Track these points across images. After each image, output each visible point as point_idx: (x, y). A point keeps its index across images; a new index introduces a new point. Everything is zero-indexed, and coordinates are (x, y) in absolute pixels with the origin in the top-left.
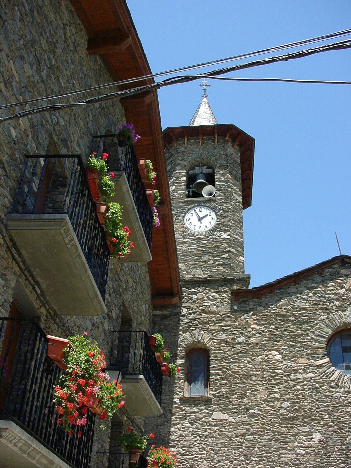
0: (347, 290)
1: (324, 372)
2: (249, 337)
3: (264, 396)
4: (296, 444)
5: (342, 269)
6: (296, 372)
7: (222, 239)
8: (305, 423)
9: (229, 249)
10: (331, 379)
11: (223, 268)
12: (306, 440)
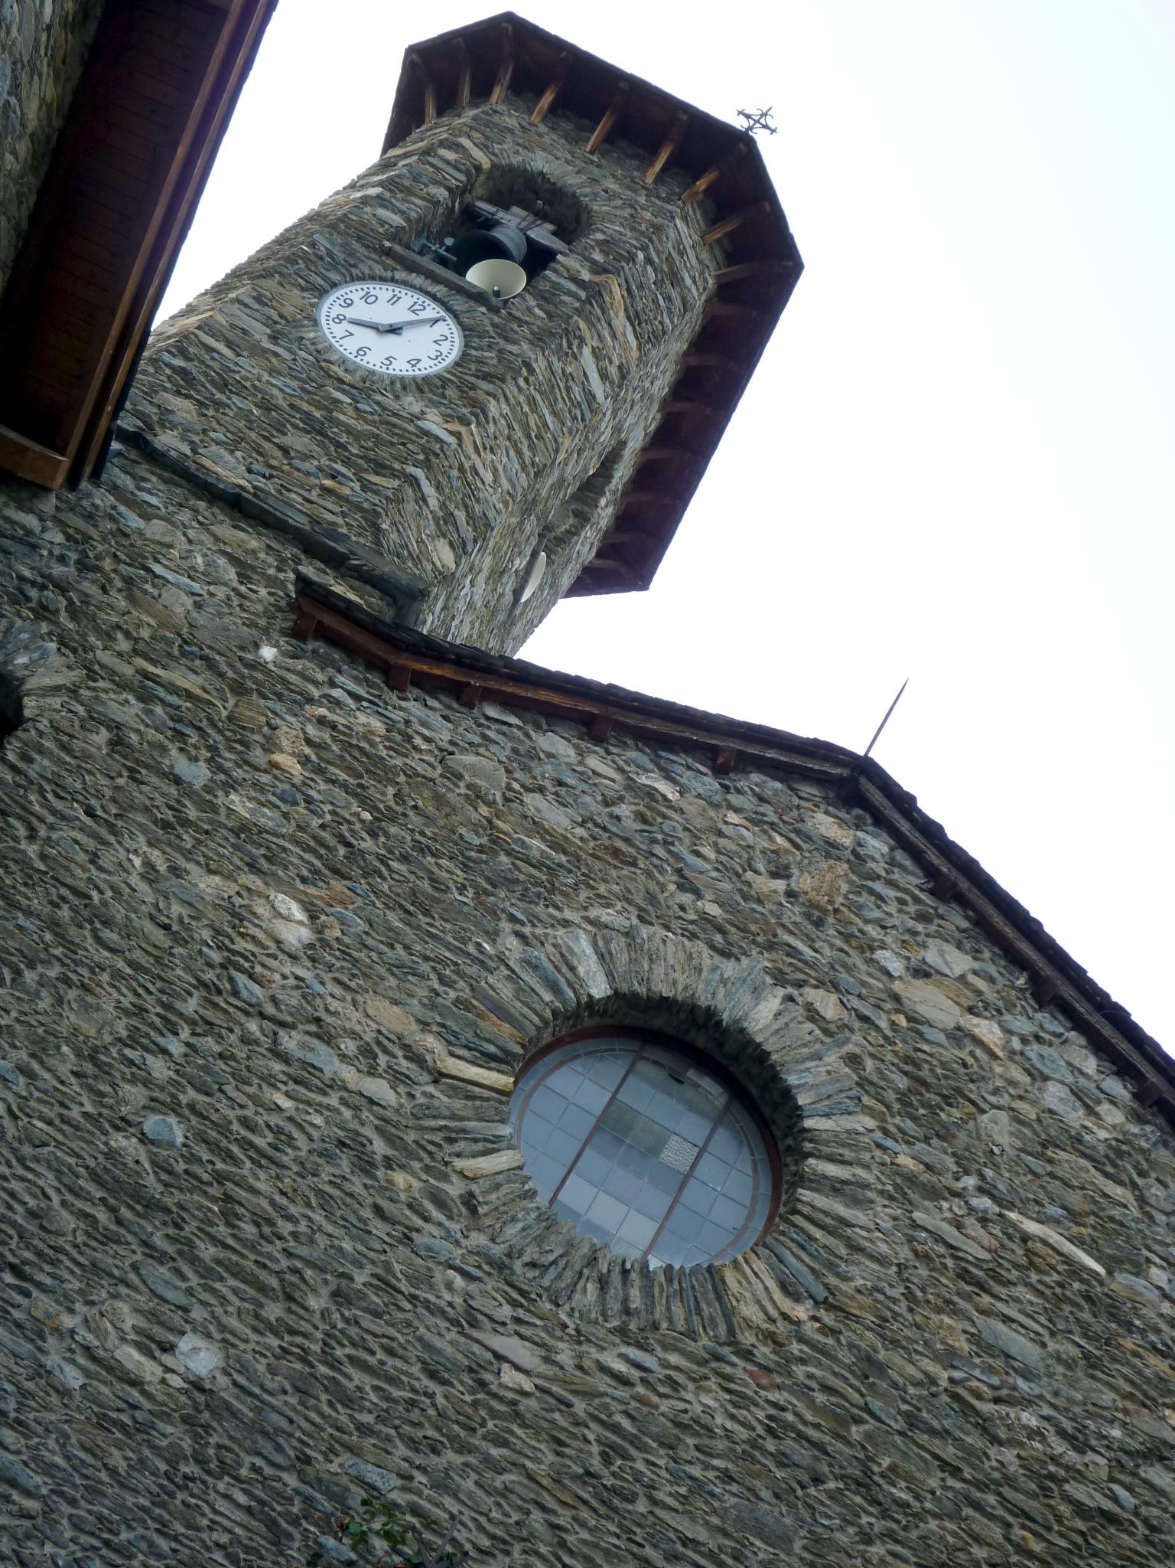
0: (790, 894)
1: (454, 1117)
2: (231, 785)
3: (92, 1033)
4: (68, 1321)
5: (827, 813)
6: (327, 1038)
7: (418, 427)
8: (194, 1261)
9: (419, 473)
10: (459, 1164)
11: (337, 509)
12: (132, 1336)
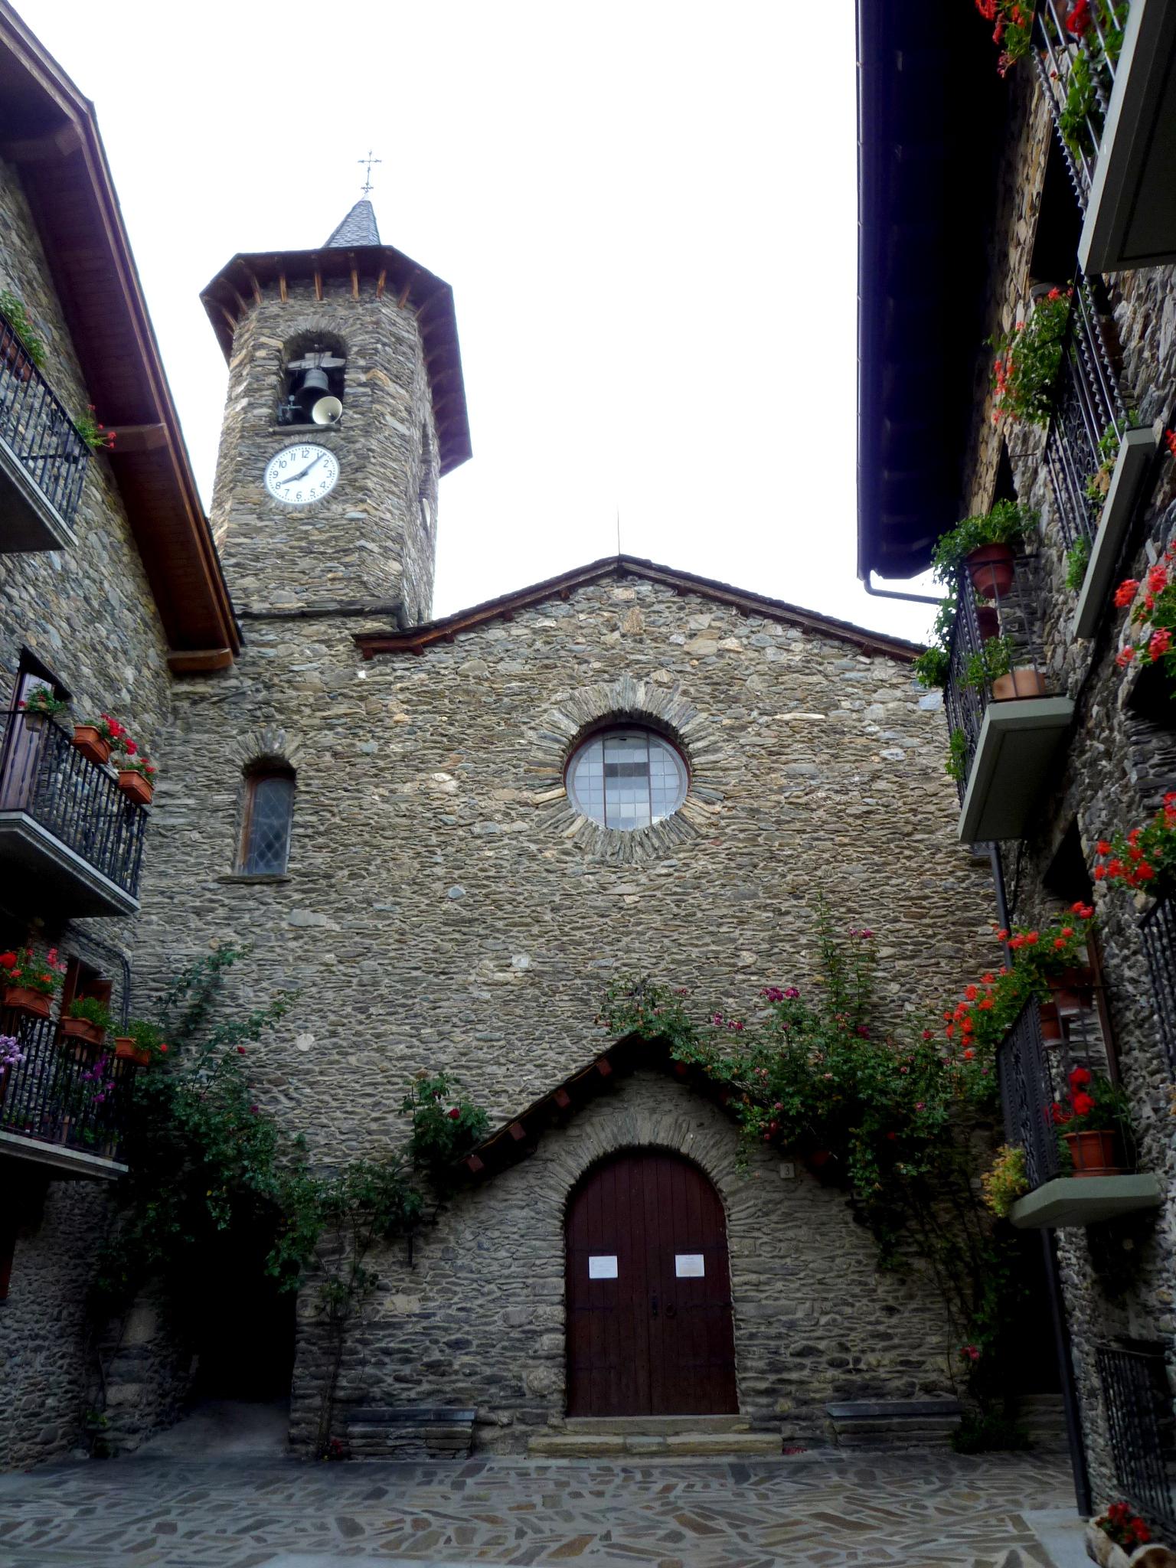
0: (623, 636)
2: (387, 743)
4: (472, 978)
6: (488, 818)
8: (498, 931)
9: (362, 542)
10: (565, 834)
